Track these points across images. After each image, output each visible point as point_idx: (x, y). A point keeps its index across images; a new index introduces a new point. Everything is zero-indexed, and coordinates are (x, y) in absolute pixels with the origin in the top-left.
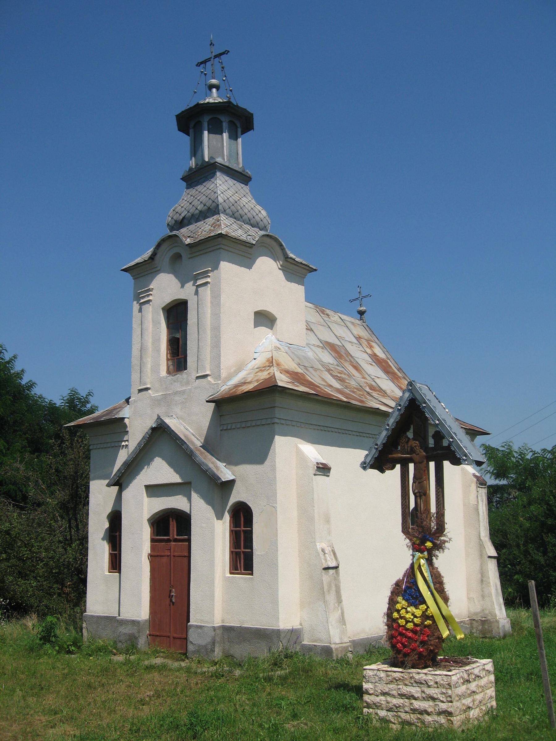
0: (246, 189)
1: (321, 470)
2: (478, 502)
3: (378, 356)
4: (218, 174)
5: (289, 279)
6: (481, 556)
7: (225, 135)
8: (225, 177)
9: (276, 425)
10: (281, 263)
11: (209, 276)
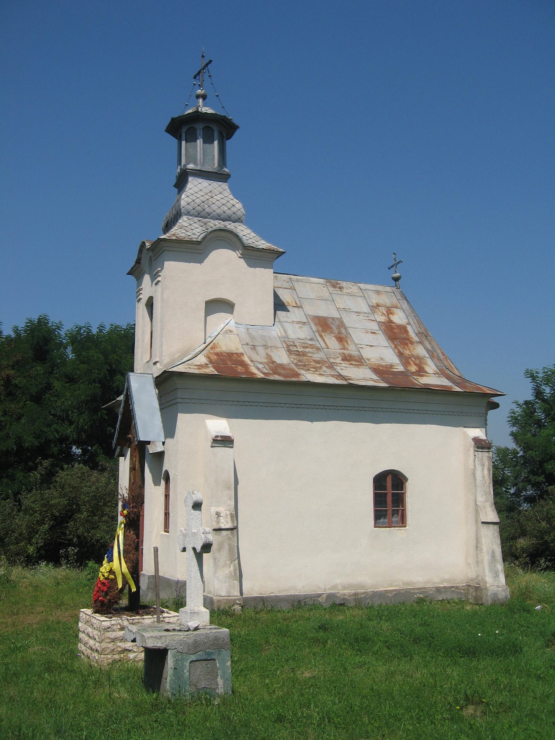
0: (225, 186)
1: (220, 442)
2: (475, 466)
3: (393, 323)
4: (190, 179)
5: (250, 265)
6: (477, 521)
7: (200, 142)
8: (197, 179)
9: (179, 405)
10: (241, 252)
11: (160, 275)
